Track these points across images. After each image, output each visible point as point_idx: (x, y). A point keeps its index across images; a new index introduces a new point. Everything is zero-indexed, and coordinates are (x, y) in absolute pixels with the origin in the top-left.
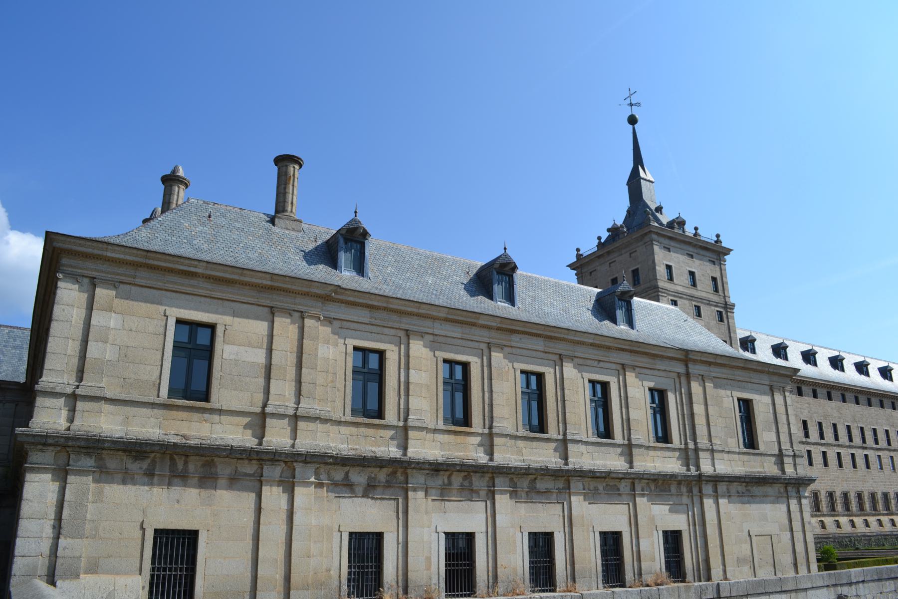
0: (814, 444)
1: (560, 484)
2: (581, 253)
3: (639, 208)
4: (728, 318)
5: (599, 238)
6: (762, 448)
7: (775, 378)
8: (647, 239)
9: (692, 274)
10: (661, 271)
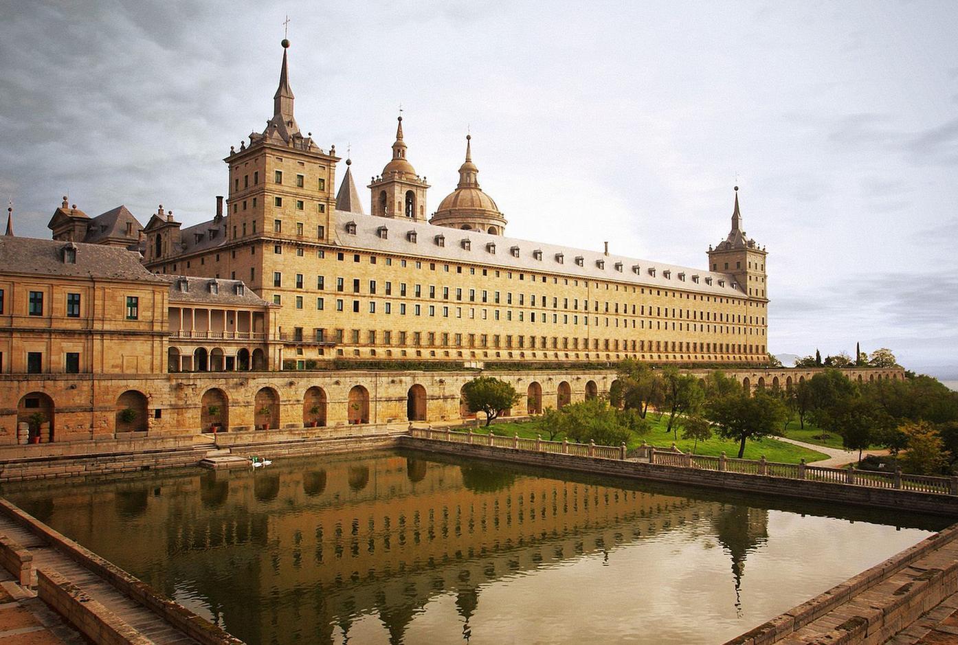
0: (394, 299)
1: (7, 335)
2: (234, 150)
3: (280, 121)
4: (328, 209)
5: (243, 143)
6: (140, 318)
7: (158, 287)
8: (262, 152)
10: (271, 176)
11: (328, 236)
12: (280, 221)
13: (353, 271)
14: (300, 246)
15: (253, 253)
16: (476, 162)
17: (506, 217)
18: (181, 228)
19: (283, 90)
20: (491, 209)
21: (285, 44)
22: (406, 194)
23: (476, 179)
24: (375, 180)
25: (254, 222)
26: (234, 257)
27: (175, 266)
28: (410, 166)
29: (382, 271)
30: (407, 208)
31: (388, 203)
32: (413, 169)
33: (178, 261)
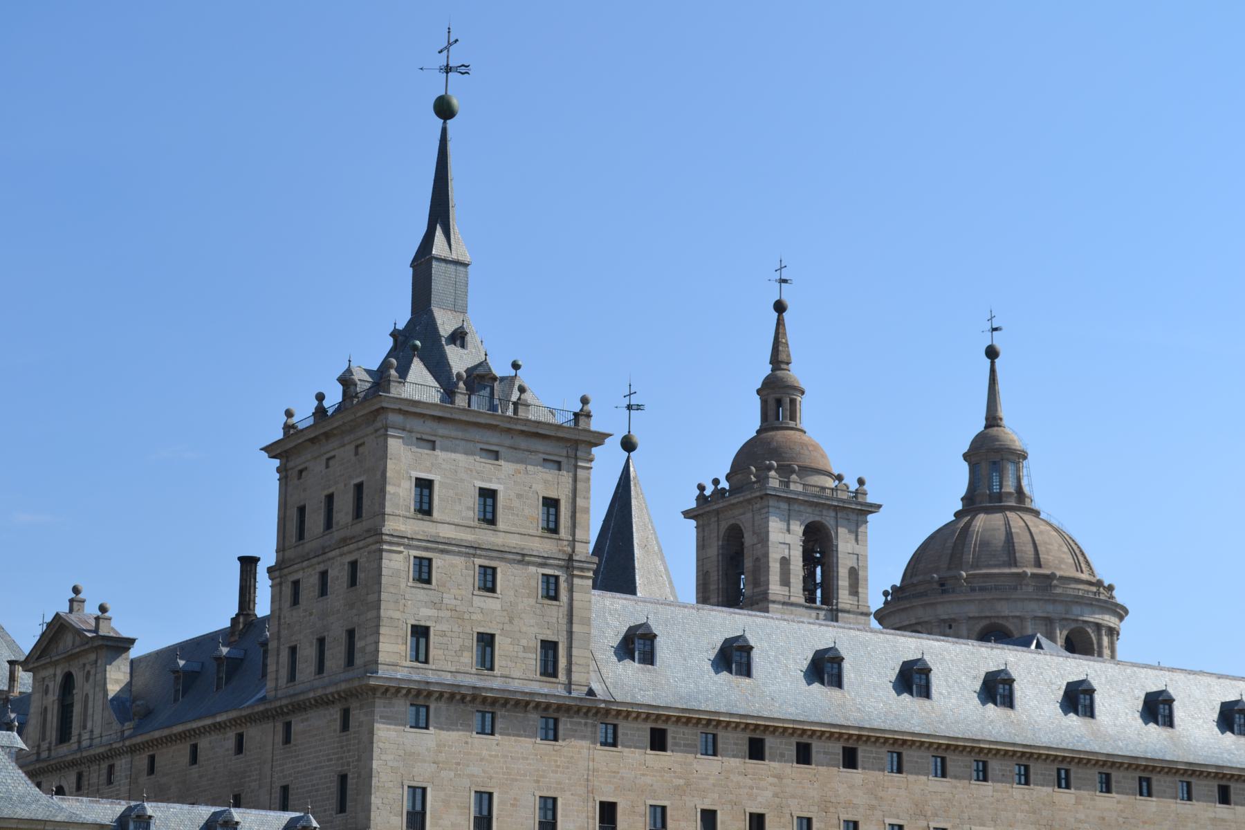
2: (294, 420)
4: (571, 590)
5: (320, 397)
8: (378, 424)
9: (488, 495)
10: (400, 493)
11: (569, 671)
12: (427, 629)
13: (648, 780)
14: (488, 710)
15: (345, 726)
16: (1015, 430)
17: (1120, 597)
18: (134, 653)
19: (439, 232)
20: (1072, 573)
21: (444, 109)
22: (804, 534)
23: (1019, 480)
24: (708, 493)
25: (351, 634)
26: (287, 740)
27: (111, 768)
28: (816, 447)
29: (735, 778)
30: (809, 578)
31: (748, 564)
32: (824, 456)
33: (117, 753)
